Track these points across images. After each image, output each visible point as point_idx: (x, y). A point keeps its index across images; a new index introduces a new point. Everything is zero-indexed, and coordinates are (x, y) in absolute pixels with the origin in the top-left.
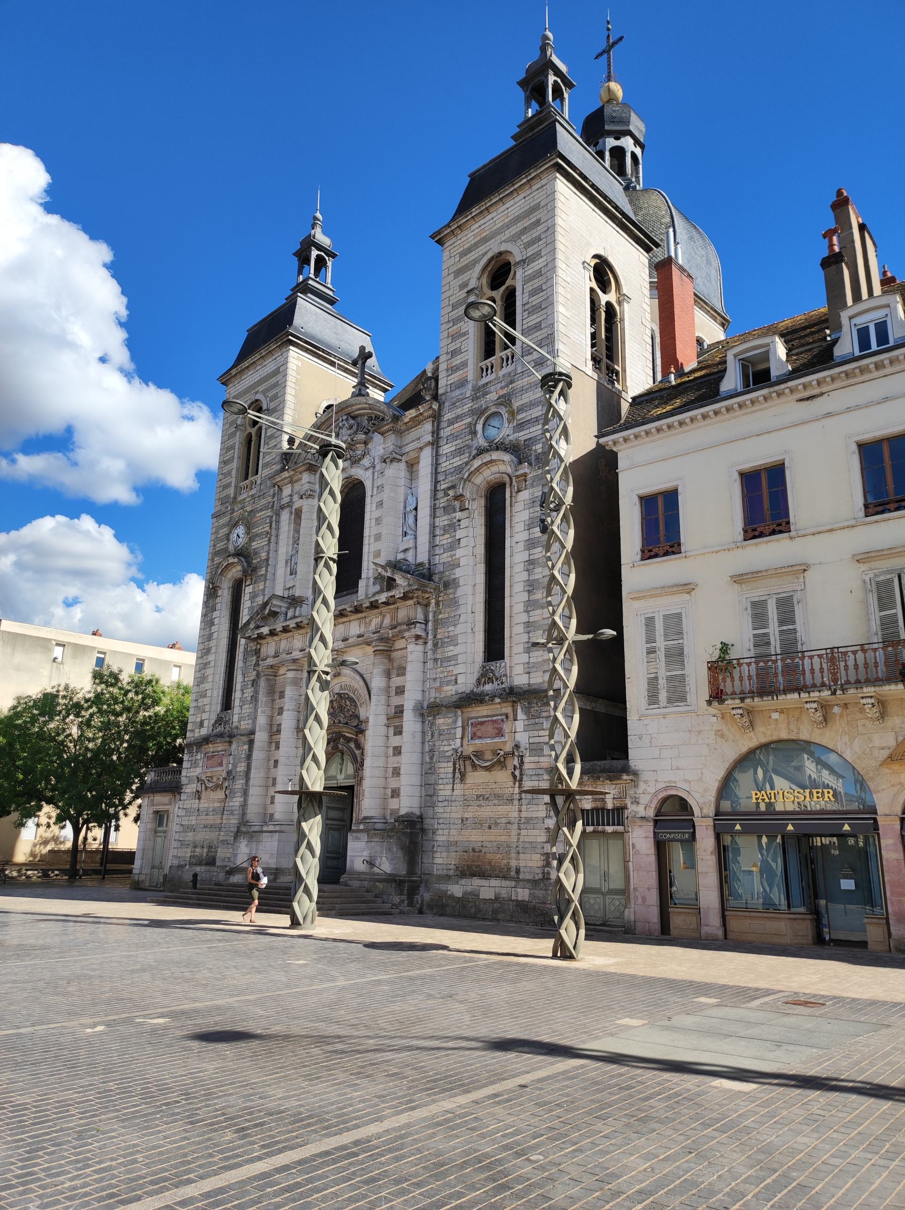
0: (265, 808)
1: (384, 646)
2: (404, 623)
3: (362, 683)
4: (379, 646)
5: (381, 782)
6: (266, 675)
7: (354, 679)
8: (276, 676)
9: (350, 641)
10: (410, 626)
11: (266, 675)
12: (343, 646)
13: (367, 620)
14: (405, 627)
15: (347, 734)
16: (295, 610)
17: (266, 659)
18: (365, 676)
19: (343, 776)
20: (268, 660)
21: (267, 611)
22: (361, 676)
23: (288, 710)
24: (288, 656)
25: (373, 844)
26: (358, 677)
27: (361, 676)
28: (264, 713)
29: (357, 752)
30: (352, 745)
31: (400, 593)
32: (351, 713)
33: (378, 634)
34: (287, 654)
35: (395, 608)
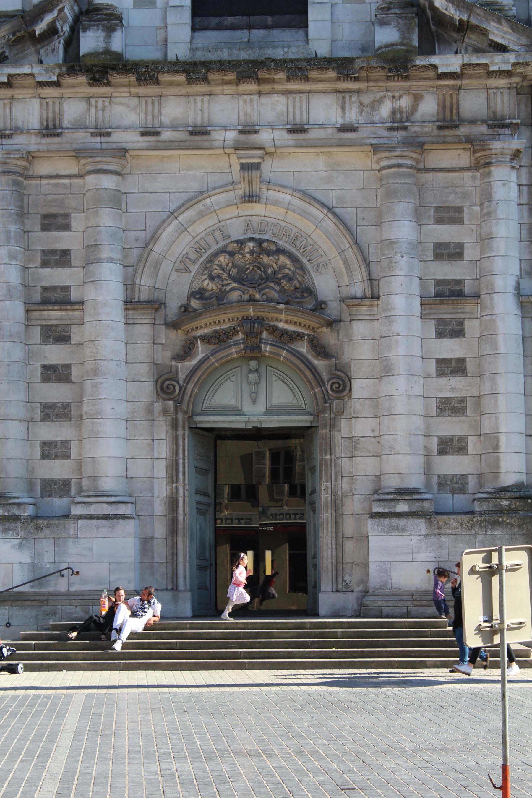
0: (32, 471)
1: (389, 158)
2: (484, 122)
3: (329, 224)
4: (408, 157)
5: (418, 423)
6: (14, 173)
7: (305, 215)
8: (27, 177)
9: (312, 135)
10: (501, 131)
11: (14, 173)
12: (291, 143)
13: (366, 99)
14: (484, 129)
15: (281, 325)
16: (108, 37)
17: (10, 136)
18: (337, 211)
19: (261, 407)
20: (19, 140)
21: (40, 28)
22: (330, 210)
23: (111, 260)
24: (98, 139)
25: (444, 539)
26: (318, 213)
27: (330, 210)
28: (15, 258)
29: (319, 363)
30: (303, 348)
31: (506, 62)
32: (296, 283)
33: (402, 133)
34: (93, 134)
35: (453, 87)
